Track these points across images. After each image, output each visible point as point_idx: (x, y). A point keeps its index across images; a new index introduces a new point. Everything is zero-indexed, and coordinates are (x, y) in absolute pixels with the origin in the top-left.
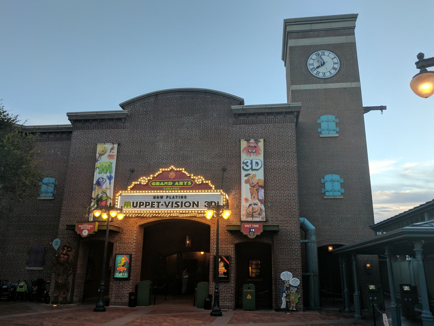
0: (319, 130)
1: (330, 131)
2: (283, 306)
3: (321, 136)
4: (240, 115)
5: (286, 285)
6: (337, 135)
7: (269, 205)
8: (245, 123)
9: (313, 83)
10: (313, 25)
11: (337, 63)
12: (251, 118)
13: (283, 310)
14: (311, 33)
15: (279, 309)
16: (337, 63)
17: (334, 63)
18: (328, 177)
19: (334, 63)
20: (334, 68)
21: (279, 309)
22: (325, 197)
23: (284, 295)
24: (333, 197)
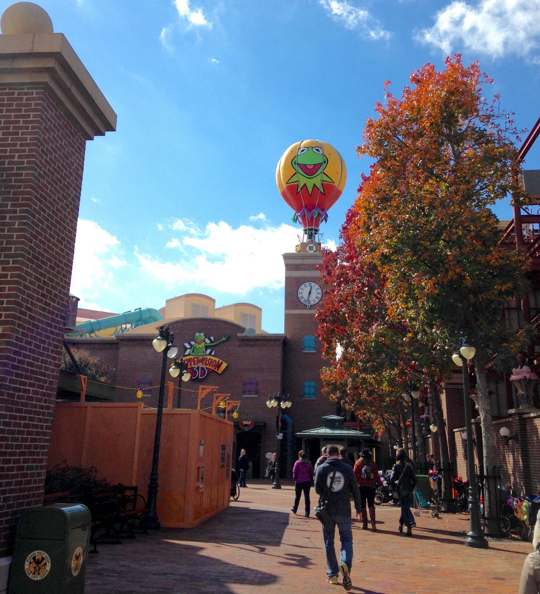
0: (303, 347)
1: (310, 348)
2: (267, 475)
3: (304, 352)
4: (243, 340)
5: (269, 461)
6: (315, 352)
7: (261, 407)
8: (247, 345)
9: (301, 309)
10: (304, 260)
11: (319, 293)
12: (252, 343)
13: (267, 478)
14: (302, 266)
15: (264, 478)
16: (319, 293)
17: (318, 293)
18: (307, 384)
19: (318, 293)
20: (317, 297)
21: (264, 478)
22: (304, 399)
23: (268, 468)
24: (309, 399)
